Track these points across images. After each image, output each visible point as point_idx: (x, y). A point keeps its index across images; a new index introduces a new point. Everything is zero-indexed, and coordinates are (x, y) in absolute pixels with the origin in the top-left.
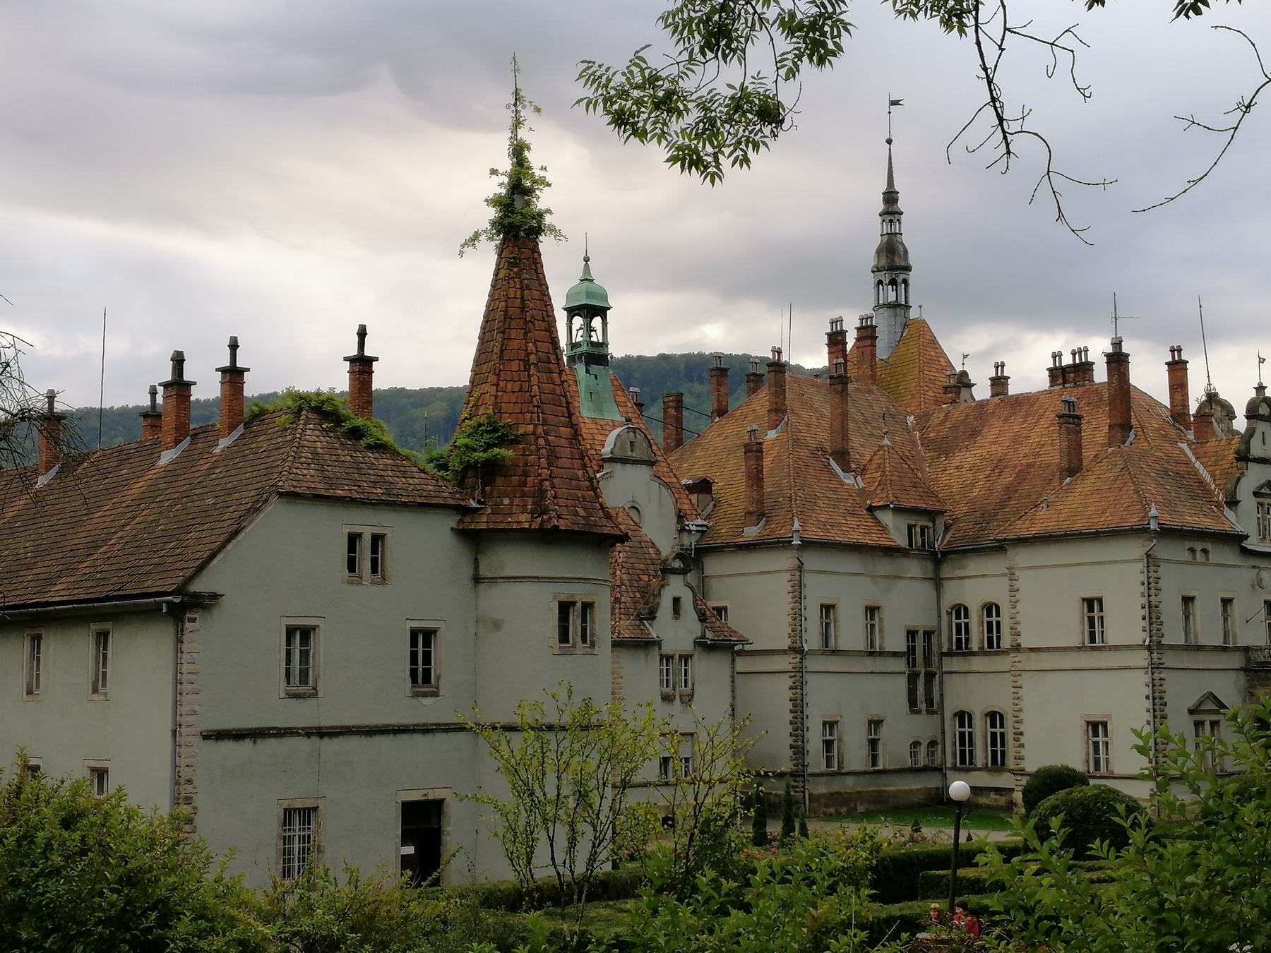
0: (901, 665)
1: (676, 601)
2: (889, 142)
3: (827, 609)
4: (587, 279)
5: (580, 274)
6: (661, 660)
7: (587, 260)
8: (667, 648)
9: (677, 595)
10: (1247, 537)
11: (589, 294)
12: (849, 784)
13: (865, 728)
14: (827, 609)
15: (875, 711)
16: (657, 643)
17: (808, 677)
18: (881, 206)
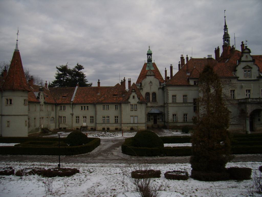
0: (192, 105)
1: (134, 97)
2: (225, 17)
3: (174, 96)
4: (149, 50)
5: (148, 49)
6: (131, 106)
7: (149, 47)
8: (131, 103)
9: (134, 95)
10: (238, 77)
11: (149, 51)
12: (179, 125)
13: (182, 116)
14: (174, 96)
15: (185, 112)
16: (130, 102)
17: (169, 107)
18: (224, 28)
